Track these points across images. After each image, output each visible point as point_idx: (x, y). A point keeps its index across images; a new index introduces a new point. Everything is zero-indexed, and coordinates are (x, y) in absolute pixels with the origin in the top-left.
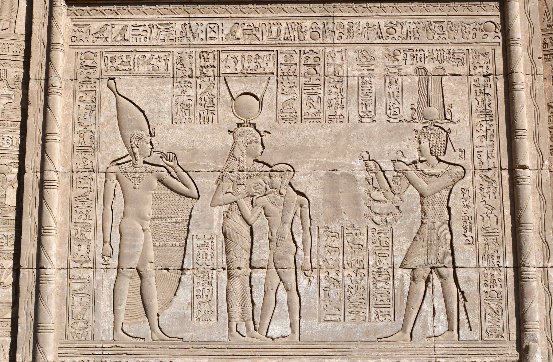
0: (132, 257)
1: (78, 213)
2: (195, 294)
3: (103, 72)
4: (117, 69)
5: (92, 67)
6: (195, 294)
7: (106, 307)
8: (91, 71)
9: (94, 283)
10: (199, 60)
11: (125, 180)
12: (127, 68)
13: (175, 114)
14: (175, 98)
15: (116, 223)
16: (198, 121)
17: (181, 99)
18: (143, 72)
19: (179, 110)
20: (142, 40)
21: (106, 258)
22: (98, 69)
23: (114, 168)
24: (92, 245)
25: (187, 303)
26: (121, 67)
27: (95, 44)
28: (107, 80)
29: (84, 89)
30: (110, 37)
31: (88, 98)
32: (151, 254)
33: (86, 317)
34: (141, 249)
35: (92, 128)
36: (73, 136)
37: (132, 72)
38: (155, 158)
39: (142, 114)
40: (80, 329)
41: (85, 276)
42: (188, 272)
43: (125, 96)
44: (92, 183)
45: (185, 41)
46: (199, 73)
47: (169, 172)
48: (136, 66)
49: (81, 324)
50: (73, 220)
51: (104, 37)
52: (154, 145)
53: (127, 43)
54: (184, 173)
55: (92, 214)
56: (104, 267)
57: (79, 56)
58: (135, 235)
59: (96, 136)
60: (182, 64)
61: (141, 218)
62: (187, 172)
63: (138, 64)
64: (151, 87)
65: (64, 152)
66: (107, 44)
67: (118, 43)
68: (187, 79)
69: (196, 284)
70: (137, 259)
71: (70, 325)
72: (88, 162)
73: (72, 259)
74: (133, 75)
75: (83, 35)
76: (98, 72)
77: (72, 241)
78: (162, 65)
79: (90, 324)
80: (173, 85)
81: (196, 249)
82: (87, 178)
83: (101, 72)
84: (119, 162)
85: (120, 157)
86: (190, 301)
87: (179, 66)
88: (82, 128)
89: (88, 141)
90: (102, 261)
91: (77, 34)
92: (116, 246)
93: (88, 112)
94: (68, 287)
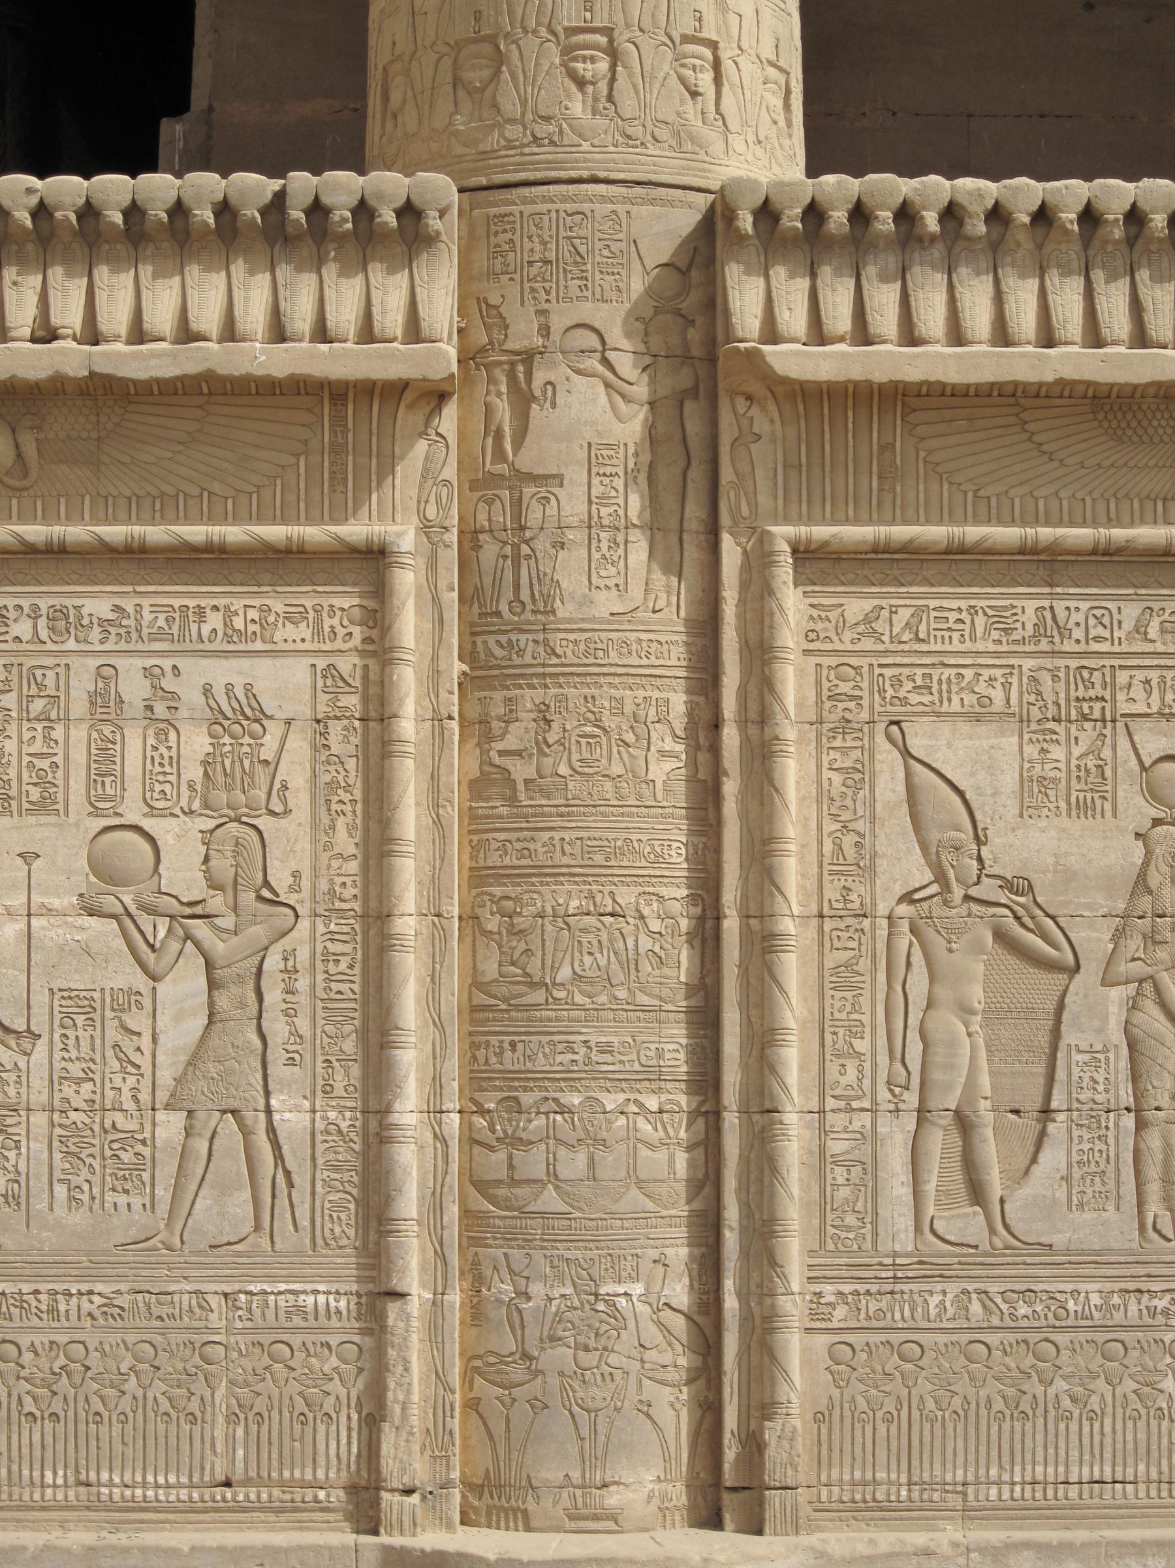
0: (948, 1087)
1: (837, 1001)
2: (1075, 1158)
3: (878, 708)
4: (904, 701)
5: (852, 698)
6: (1075, 1158)
7: (898, 1186)
8: (852, 705)
9: (872, 1138)
10: (1073, 686)
11: (930, 934)
12: (926, 699)
13: (1026, 800)
14: (1026, 765)
15: (913, 1021)
16: (1074, 813)
17: (1038, 768)
18: (959, 709)
19: (1036, 789)
20: (955, 641)
21: (897, 1090)
22: (865, 703)
23: (904, 909)
24: (867, 1065)
25: (1058, 1176)
26: (914, 698)
27: (857, 647)
28: (884, 725)
29: (838, 743)
30: (887, 633)
31: (848, 763)
32: (985, 1081)
33: (859, 1206)
34: (965, 1072)
35: (860, 826)
36: (820, 843)
37: (937, 709)
38: (988, 889)
39: (957, 800)
40: (849, 1229)
41: (856, 1125)
42: (1061, 1117)
43: (925, 760)
44: (864, 939)
45: (1044, 645)
46: (1073, 712)
47: (1017, 918)
48: (945, 695)
49: (851, 1220)
50: (828, 1015)
51: (875, 631)
52: (987, 863)
53: (924, 647)
54: (1048, 920)
55: (865, 1001)
56: (892, 1107)
57: (825, 672)
58: (953, 1044)
59: (867, 842)
60: (1039, 693)
61: (965, 1011)
62: (1053, 918)
63: (949, 691)
64: (977, 743)
65: (803, 876)
66: (881, 647)
67: (906, 647)
68: (1051, 725)
69: (1076, 1140)
70: (958, 1093)
71: (829, 1222)
72: (853, 896)
73: (829, 1092)
74: (939, 714)
75: (831, 626)
76: (866, 709)
77: (828, 1057)
78: (998, 694)
79: (868, 1219)
80: (1021, 736)
81: (1076, 1071)
82: (852, 930)
83: (871, 708)
84: (917, 896)
85: (917, 885)
86: (1064, 1172)
87: (1032, 698)
88: (838, 826)
89: (850, 852)
90: (890, 1097)
91: (819, 626)
92: (915, 1066)
93: (849, 792)
94: (822, 1149)
